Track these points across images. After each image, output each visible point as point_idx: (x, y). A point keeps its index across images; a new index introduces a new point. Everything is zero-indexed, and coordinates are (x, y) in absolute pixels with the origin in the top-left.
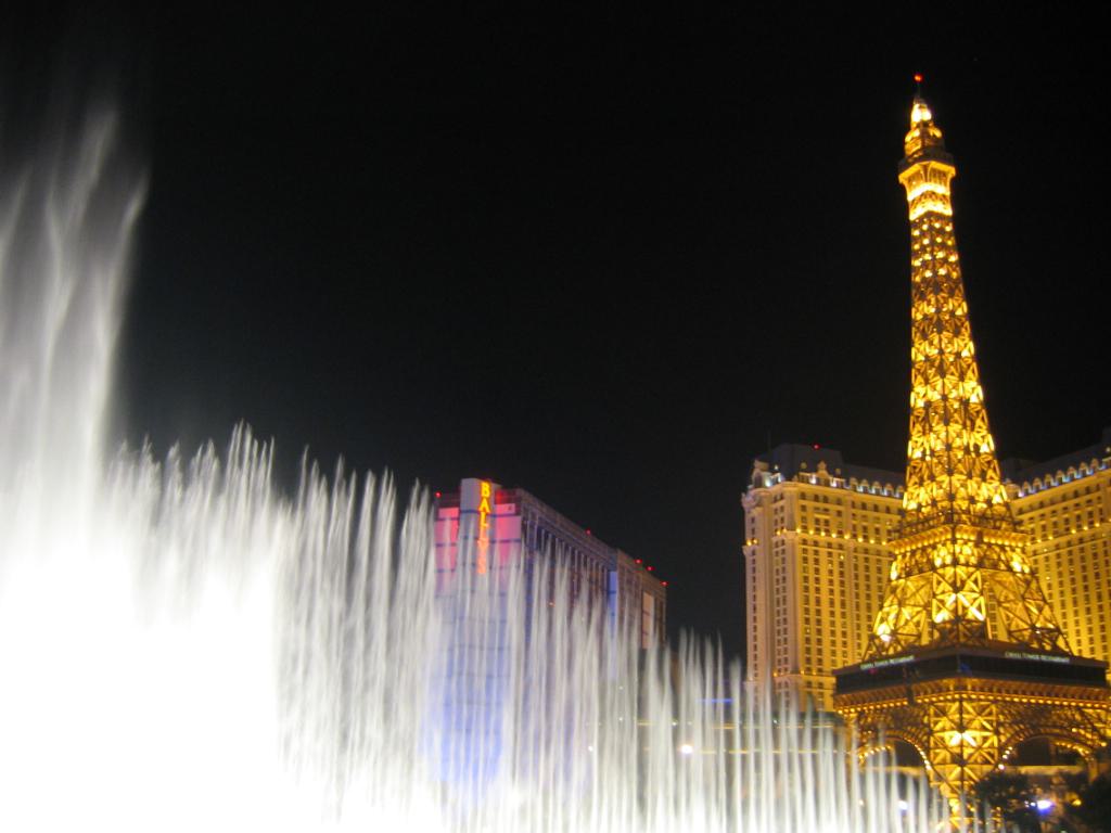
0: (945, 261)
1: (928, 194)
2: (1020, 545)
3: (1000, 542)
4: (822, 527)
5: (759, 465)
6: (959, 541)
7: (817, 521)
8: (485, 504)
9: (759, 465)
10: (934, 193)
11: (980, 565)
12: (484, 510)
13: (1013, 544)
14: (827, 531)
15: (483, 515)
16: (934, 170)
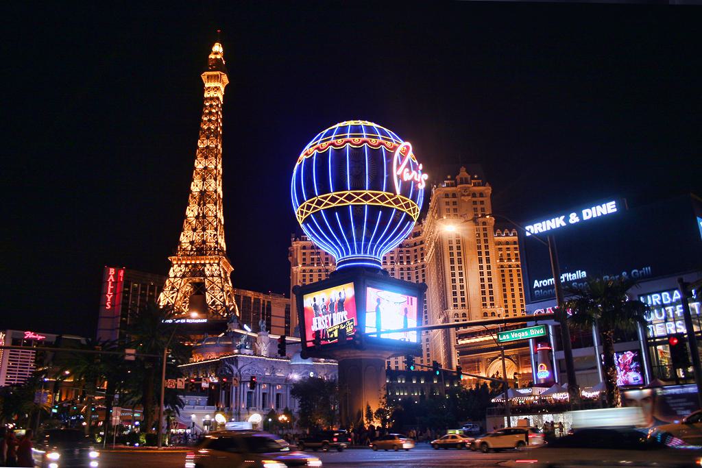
0: (210, 120)
1: (215, 88)
2: (217, 262)
3: (203, 262)
4: (316, 262)
5: (293, 235)
6: (176, 266)
7: (313, 259)
8: (111, 277)
9: (293, 235)
10: (209, 88)
11: (183, 276)
12: (111, 280)
13: (212, 262)
14: (318, 264)
15: (110, 282)
16: (211, 76)
